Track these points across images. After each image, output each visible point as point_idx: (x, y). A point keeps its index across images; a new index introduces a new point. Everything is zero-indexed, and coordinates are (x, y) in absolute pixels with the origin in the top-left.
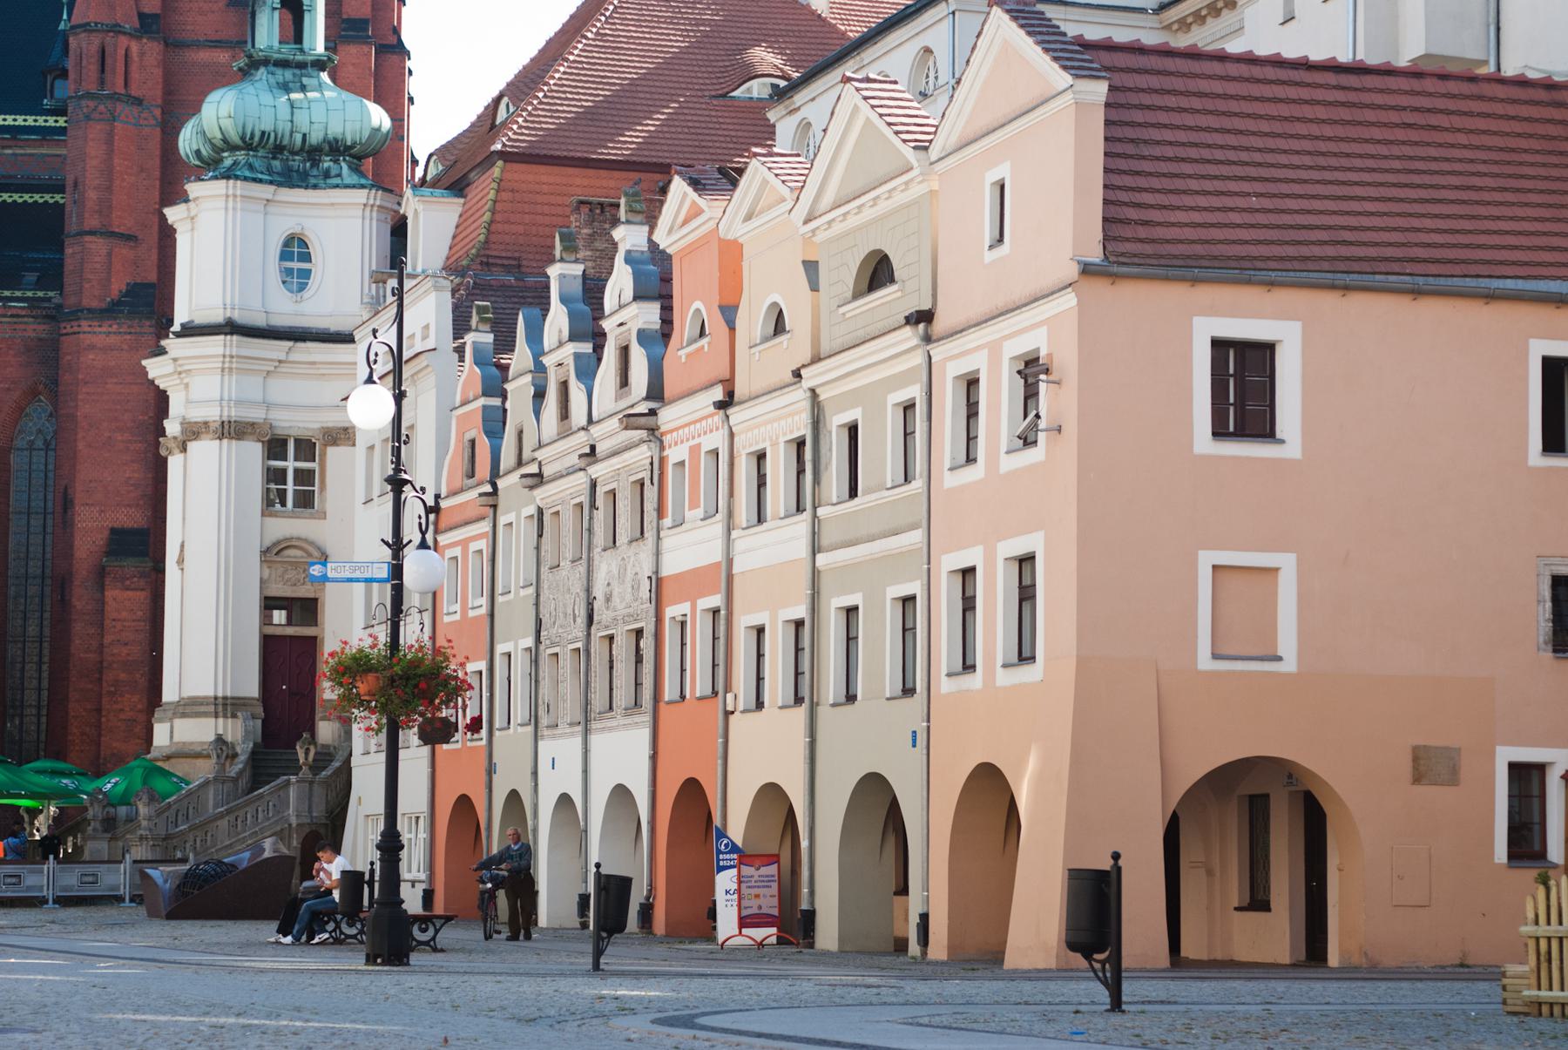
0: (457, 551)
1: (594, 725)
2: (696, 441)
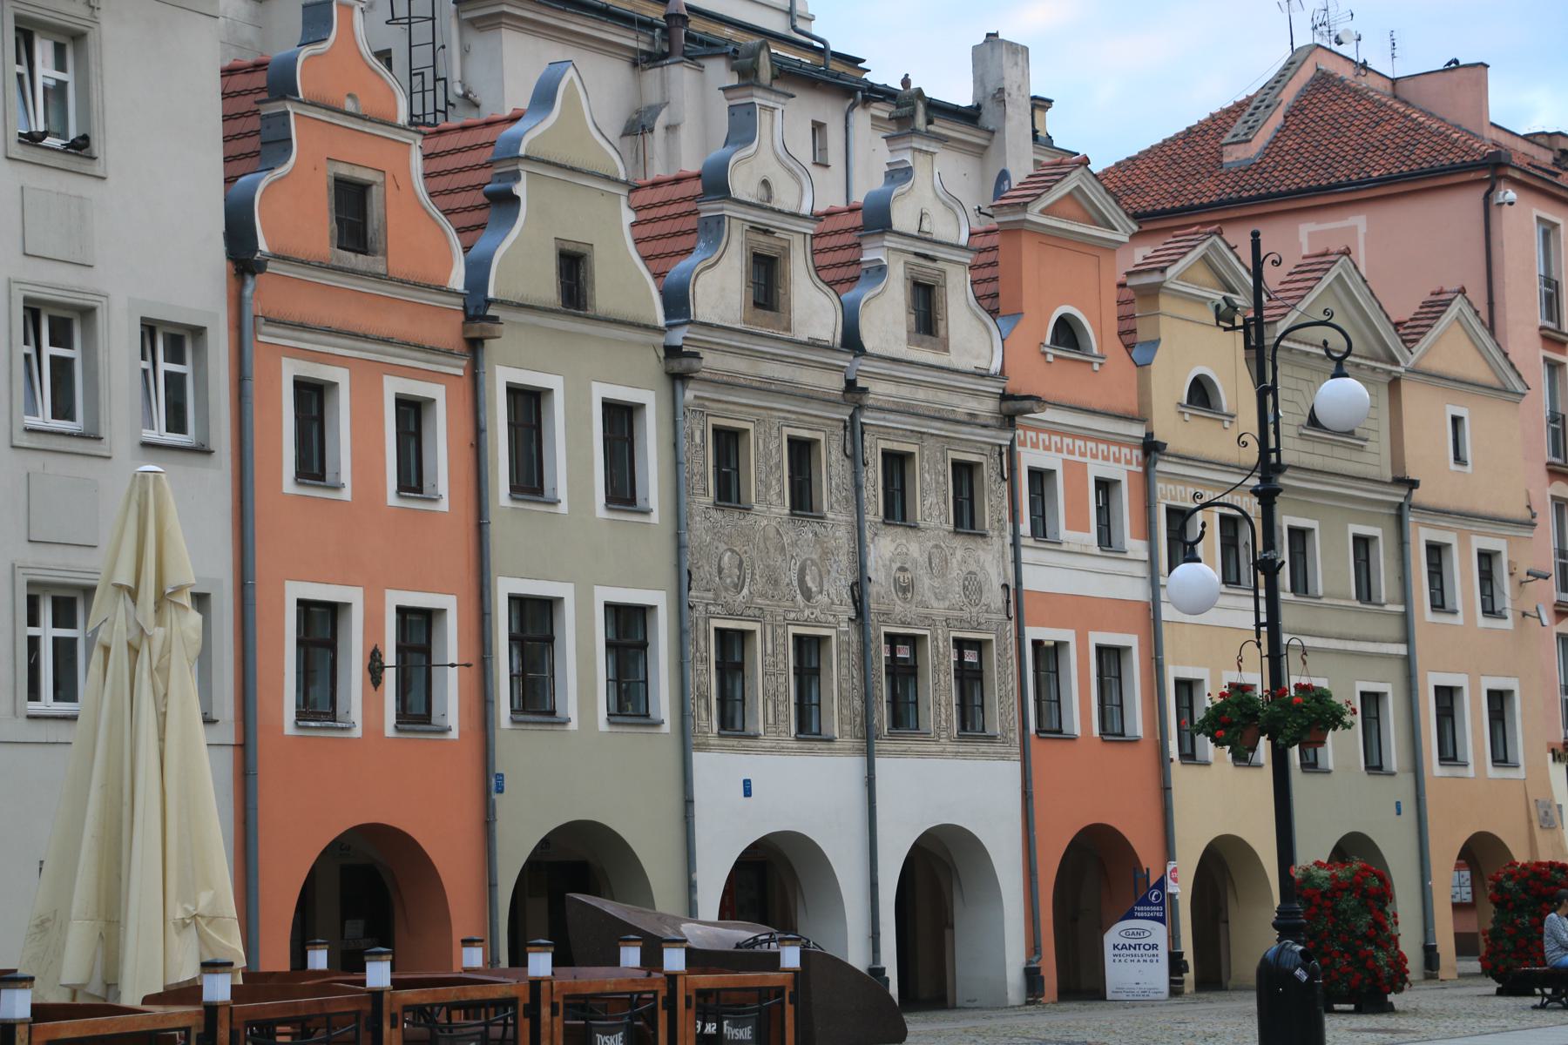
0: (340, 376)
1: (879, 745)
2: (1077, 458)
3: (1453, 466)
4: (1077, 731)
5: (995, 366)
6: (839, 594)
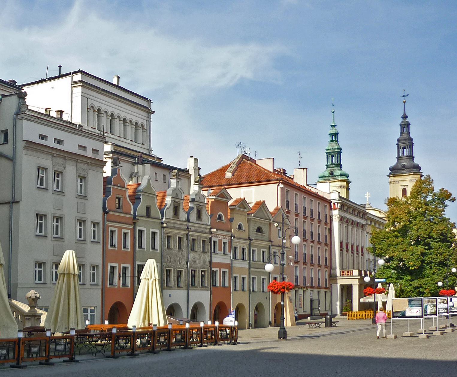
0: (116, 229)
1: (190, 288)
2: (220, 239)
3: (278, 238)
4: (218, 286)
5: (209, 223)
6: (184, 263)
